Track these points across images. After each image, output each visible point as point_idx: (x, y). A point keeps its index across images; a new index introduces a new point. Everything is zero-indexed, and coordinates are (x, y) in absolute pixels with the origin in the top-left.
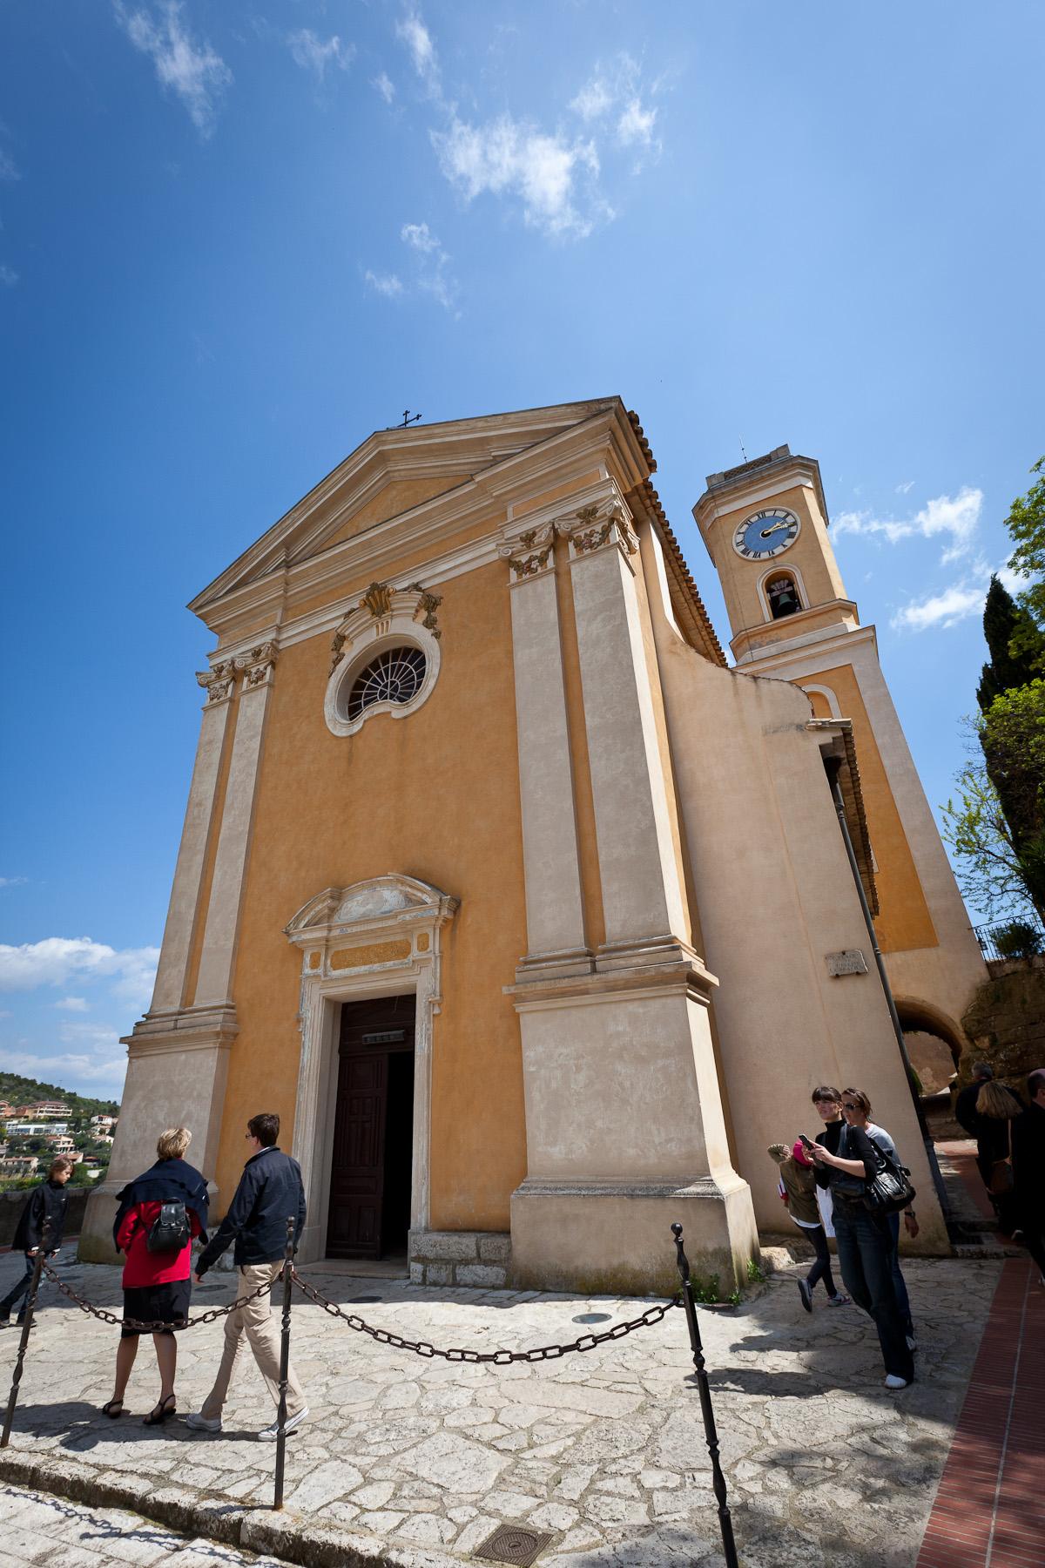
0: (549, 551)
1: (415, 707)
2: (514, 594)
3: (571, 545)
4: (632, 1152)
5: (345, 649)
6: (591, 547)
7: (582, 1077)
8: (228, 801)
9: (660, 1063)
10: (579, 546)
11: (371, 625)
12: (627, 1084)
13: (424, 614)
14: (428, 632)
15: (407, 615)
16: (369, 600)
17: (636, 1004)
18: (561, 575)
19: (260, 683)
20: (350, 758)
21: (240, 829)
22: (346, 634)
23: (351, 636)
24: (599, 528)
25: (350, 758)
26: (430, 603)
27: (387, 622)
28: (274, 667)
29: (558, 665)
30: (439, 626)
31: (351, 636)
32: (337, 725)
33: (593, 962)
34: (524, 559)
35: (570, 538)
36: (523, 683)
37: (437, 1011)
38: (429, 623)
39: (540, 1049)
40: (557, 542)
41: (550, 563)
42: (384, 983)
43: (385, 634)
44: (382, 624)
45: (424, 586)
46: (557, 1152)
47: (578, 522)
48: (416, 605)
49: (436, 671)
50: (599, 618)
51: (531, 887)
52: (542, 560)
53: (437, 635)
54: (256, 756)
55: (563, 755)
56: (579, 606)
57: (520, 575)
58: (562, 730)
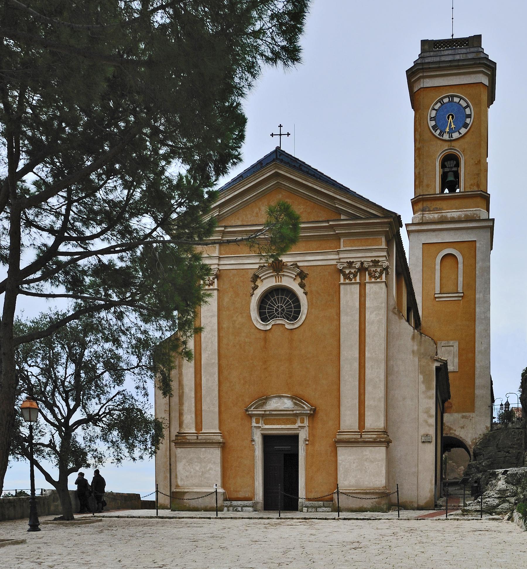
0: (358, 272)
1: (296, 326)
2: (342, 287)
3: (367, 273)
4: (366, 483)
5: (258, 282)
6: (375, 278)
7: (355, 465)
8: (203, 346)
9: (377, 463)
10: (371, 276)
11: (272, 276)
12: (367, 467)
13: (299, 280)
14: (302, 290)
15: (292, 277)
16: (273, 264)
17: (372, 447)
18: (362, 286)
19: (211, 287)
20: (265, 340)
21: (213, 361)
22: (260, 276)
23: (262, 278)
24: (379, 270)
25: (265, 340)
26: (302, 275)
27: (281, 277)
28: (217, 280)
29: (357, 328)
30: (307, 289)
31: (262, 278)
32: (260, 325)
33: (361, 435)
34: (347, 271)
35: (366, 269)
36: (343, 330)
37: (307, 443)
38: (302, 286)
39: (343, 457)
40: (362, 269)
41: (358, 278)
42: (286, 432)
43: (280, 284)
44: (278, 277)
45: (299, 264)
46: (346, 483)
47: (371, 264)
48: (296, 274)
49: (306, 311)
50: (375, 313)
51: (342, 409)
52: (355, 276)
53: (306, 293)
54: (216, 327)
55: (356, 365)
56: (367, 305)
57: (345, 279)
58: (357, 355)
